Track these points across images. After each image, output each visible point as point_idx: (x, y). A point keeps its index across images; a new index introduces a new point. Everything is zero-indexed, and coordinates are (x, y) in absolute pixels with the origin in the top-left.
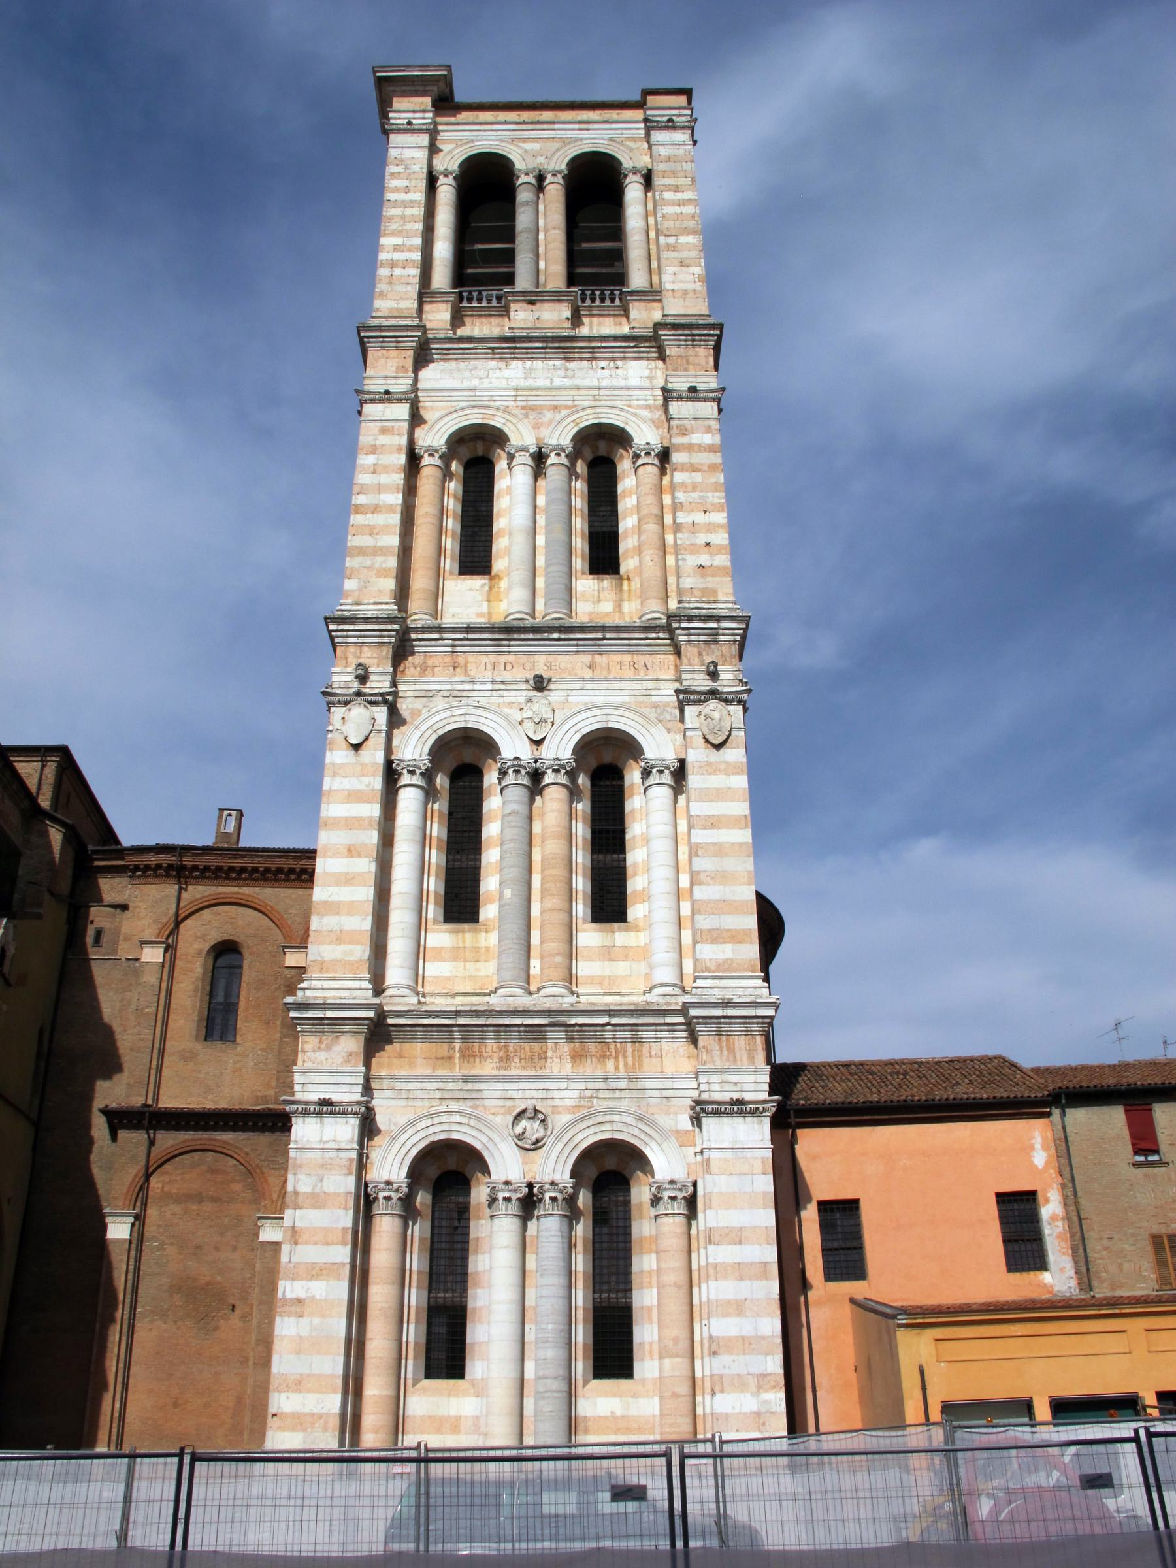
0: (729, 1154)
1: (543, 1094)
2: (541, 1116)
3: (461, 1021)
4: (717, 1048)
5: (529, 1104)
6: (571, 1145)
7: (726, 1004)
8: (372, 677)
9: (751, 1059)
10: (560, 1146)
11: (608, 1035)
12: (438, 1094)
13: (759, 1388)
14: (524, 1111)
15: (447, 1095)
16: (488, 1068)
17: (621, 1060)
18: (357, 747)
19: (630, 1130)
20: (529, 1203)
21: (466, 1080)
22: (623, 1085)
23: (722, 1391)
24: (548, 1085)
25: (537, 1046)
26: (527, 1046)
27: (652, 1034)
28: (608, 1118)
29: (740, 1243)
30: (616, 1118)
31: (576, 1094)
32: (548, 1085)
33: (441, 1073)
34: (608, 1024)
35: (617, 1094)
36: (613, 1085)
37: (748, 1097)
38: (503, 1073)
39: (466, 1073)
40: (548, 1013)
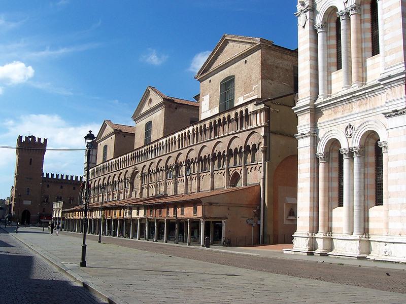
0: (394, 129)
1: (353, 120)
2: (351, 127)
3: (331, 102)
4: (391, 92)
5: (347, 124)
6: (359, 134)
7: (390, 77)
8: (306, 3)
9: (401, 93)
10: (356, 135)
11: (367, 96)
12: (329, 126)
13: (401, 208)
14: (347, 127)
15: (332, 125)
16: (339, 115)
17: (371, 103)
18: (304, 27)
19: (375, 126)
20: (351, 155)
21: (334, 120)
22: (371, 112)
23: (391, 209)
24: (354, 116)
25: (350, 105)
26: (348, 105)
27: (378, 93)
28: (368, 124)
29: (397, 160)
30: (370, 123)
31: (360, 118)
32: (354, 116)
33: (330, 119)
34: (365, 93)
35: (370, 115)
36: (369, 112)
37: (398, 109)
38: (343, 115)
39: (335, 118)
40: (350, 94)
